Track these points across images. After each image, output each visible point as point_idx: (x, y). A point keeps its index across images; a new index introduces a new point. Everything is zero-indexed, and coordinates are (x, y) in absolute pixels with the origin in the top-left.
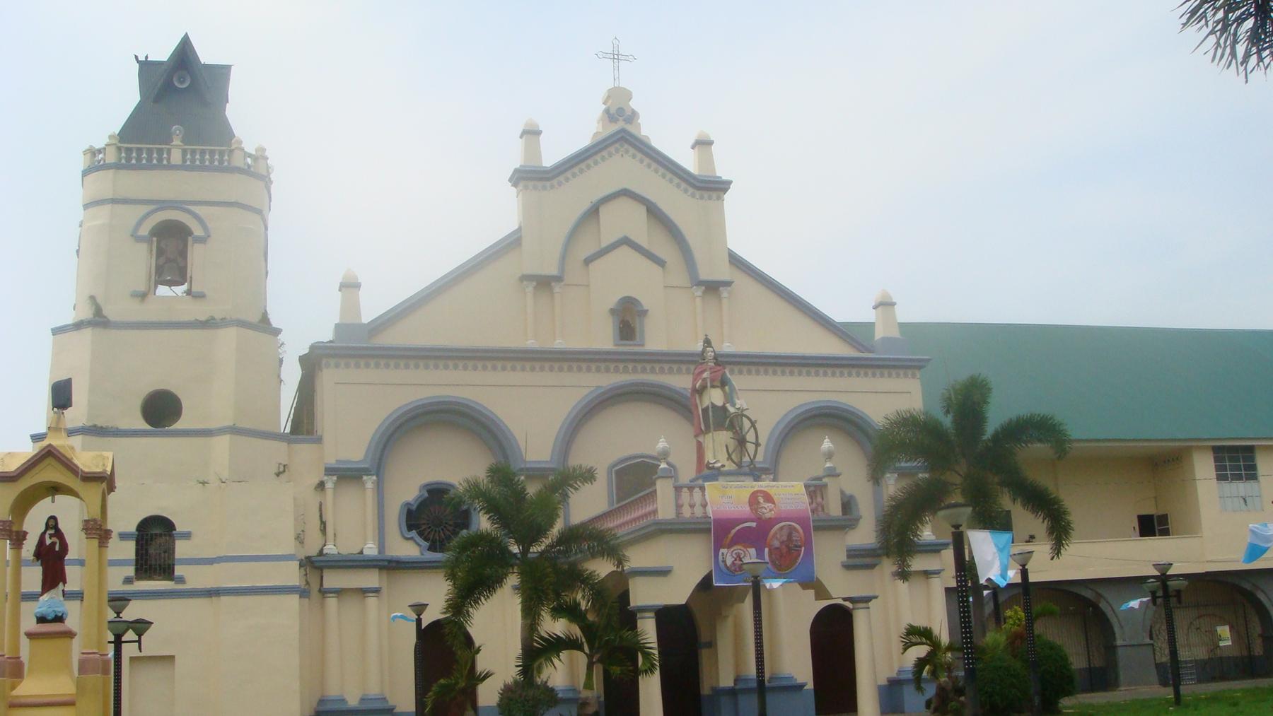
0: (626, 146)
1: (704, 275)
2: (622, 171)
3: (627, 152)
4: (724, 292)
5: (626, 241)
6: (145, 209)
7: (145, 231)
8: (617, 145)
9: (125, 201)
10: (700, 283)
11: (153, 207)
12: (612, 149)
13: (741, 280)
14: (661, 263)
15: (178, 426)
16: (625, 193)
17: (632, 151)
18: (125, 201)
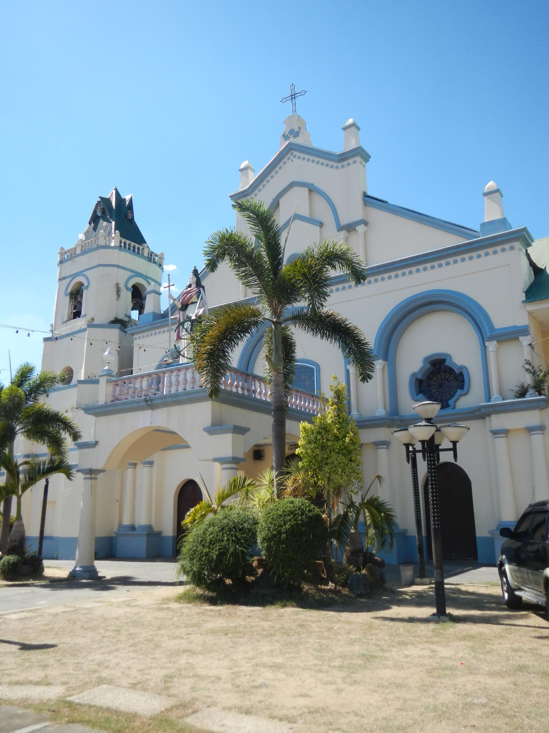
0: (295, 153)
1: (344, 221)
2: (297, 169)
3: (295, 156)
4: (361, 229)
5: (297, 217)
6: (69, 279)
7: (69, 290)
8: (289, 155)
9: (64, 278)
10: (340, 228)
11: (71, 278)
12: (285, 159)
13: (377, 216)
14: (321, 225)
15: (71, 384)
16: (293, 185)
17: (298, 154)
18: (64, 278)
